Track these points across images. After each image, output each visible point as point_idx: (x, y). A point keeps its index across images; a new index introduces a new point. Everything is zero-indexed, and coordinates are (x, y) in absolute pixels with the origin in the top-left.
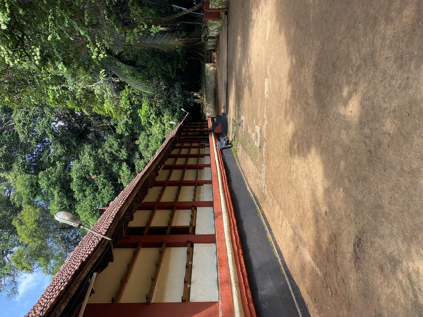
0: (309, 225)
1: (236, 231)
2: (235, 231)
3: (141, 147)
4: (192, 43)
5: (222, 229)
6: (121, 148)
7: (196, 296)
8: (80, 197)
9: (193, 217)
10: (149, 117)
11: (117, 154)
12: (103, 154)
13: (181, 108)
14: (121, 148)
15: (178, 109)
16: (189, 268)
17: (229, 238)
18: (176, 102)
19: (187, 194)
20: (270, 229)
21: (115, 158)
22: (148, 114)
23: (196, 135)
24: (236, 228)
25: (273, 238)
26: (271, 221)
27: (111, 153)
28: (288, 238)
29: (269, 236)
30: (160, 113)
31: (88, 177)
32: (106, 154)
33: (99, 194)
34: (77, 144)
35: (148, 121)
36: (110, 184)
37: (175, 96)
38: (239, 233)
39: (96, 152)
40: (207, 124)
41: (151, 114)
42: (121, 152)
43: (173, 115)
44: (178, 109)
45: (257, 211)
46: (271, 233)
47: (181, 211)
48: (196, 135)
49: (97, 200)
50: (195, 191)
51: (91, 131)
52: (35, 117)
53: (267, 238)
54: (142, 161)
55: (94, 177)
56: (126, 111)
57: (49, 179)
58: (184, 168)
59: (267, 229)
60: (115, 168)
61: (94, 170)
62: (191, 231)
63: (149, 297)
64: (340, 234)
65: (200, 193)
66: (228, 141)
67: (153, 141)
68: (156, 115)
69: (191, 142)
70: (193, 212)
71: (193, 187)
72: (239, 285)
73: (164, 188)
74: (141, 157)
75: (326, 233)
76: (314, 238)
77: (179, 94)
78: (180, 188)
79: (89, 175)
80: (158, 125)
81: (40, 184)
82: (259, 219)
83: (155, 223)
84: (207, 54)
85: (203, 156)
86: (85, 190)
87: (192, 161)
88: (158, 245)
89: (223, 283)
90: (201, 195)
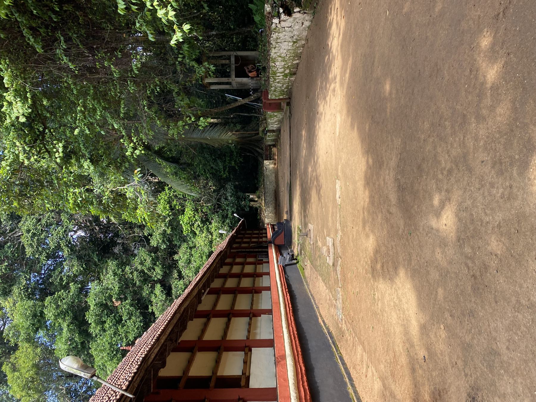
1: (306, 384)
2: (303, 383)
3: (181, 264)
4: (248, 137)
5: (286, 380)
6: (155, 264)
8: (97, 331)
9: (247, 363)
10: (193, 225)
11: (149, 273)
12: (132, 273)
13: (233, 213)
14: (155, 264)
15: (230, 214)
17: (296, 393)
18: (228, 206)
19: (238, 331)
20: (351, 379)
21: (146, 278)
22: (192, 221)
23: (251, 248)
24: (305, 378)
25: (356, 392)
26: (352, 368)
27: (143, 271)
28: (376, 393)
29: (351, 391)
30: (207, 220)
31: (109, 304)
33: (123, 326)
34: (99, 260)
35: (191, 229)
36: (138, 314)
37: (226, 199)
38: (309, 385)
39: (123, 271)
40: (266, 233)
41: (196, 220)
42: (154, 270)
43: (224, 222)
44: (230, 214)
45: (332, 353)
46: (353, 386)
47: (231, 353)
48: (251, 248)
49: (119, 335)
50: (250, 324)
51: (119, 243)
52: (48, 225)
53: (348, 393)
54: (181, 282)
55: (117, 304)
57: (58, 307)
58: (235, 292)
59: (347, 380)
60: (145, 292)
61: (119, 294)
62: (243, 383)
65: (256, 328)
66: (293, 255)
67: (196, 255)
68: (202, 222)
69: (245, 257)
70: (246, 354)
71: (247, 319)
73: (209, 320)
74: (181, 277)
77: (231, 196)
78: (229, 320)
79: (111, 301)
80: (204, 235)
81: (46, 313)
82: (336, 364)
83: (194, 372)
84: (266, 149)
85: (260, 275)
86: (105, 322)
87: (246, 283)
90: (258, 331)
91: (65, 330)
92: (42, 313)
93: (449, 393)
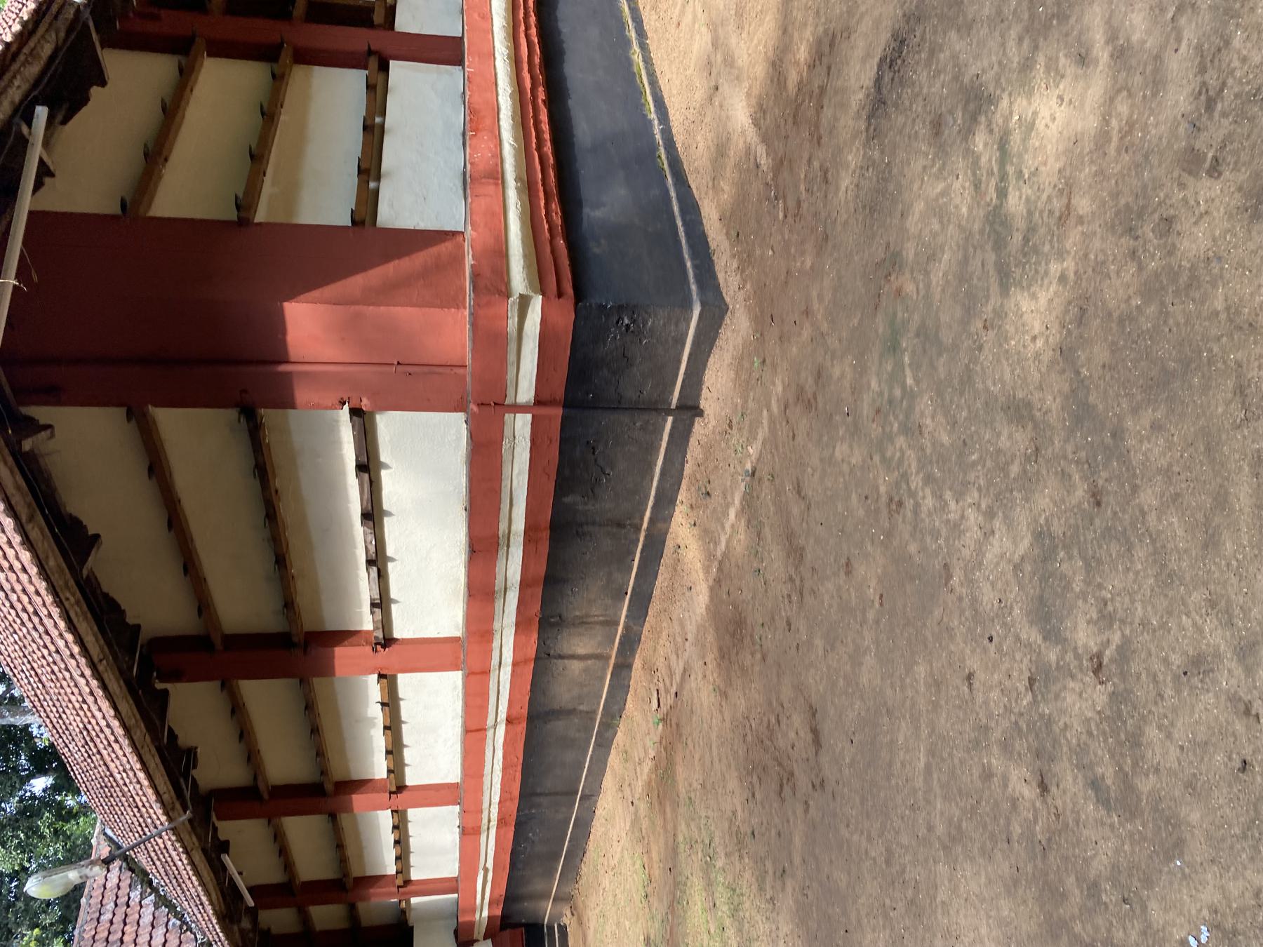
0: (761, 11)
1: (534, 31)
2: (527, 28)
5: (487, 17)
7: (400, 208)
16: (373, 133)
17: (508, 47)
20: (641, 34)
24: (533, 19)
25: (648, 61)
26: (648, 7)
28: (693, 62)
29: (637, 57)
38: (541, 36)
46: (644, 47)
53: (629, 63)
59: (633, 35)
62: (378, 17)
63: (245, 204)
64: (848, 31)
72: (528, 188)
75: (808, 33)
76: (770, 54)
88: (266, 53)
89: (479, 180)
93: (852, 38)
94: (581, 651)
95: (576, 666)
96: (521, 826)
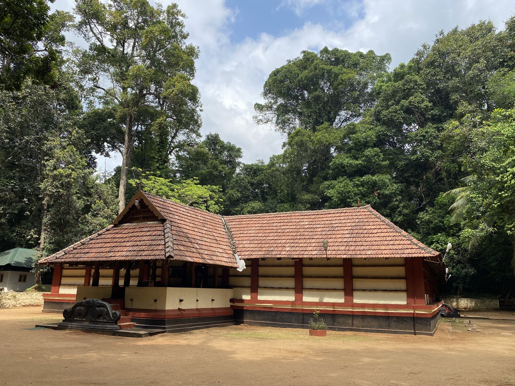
6: (404, 215)
10: (438, 243)
12: (397, 200)
18: (457, 269)
27: (398, 207)
31: (376, 188)
32: (397, 203)
33: (360, 198)
35: (435, 242)
37: (463, 268)
39: (398, 194)
41: (442, 245)
42: (400, 215)
51: (418, 189)
52: (431, 143)
56: (443, 222)
61: (383, 194)
77: (465, 272)
86: (363, 187)
91: (357, 162)
92: (369, 147)
94: (354, 322)
95: (350, 321)
96: (291, 313)
